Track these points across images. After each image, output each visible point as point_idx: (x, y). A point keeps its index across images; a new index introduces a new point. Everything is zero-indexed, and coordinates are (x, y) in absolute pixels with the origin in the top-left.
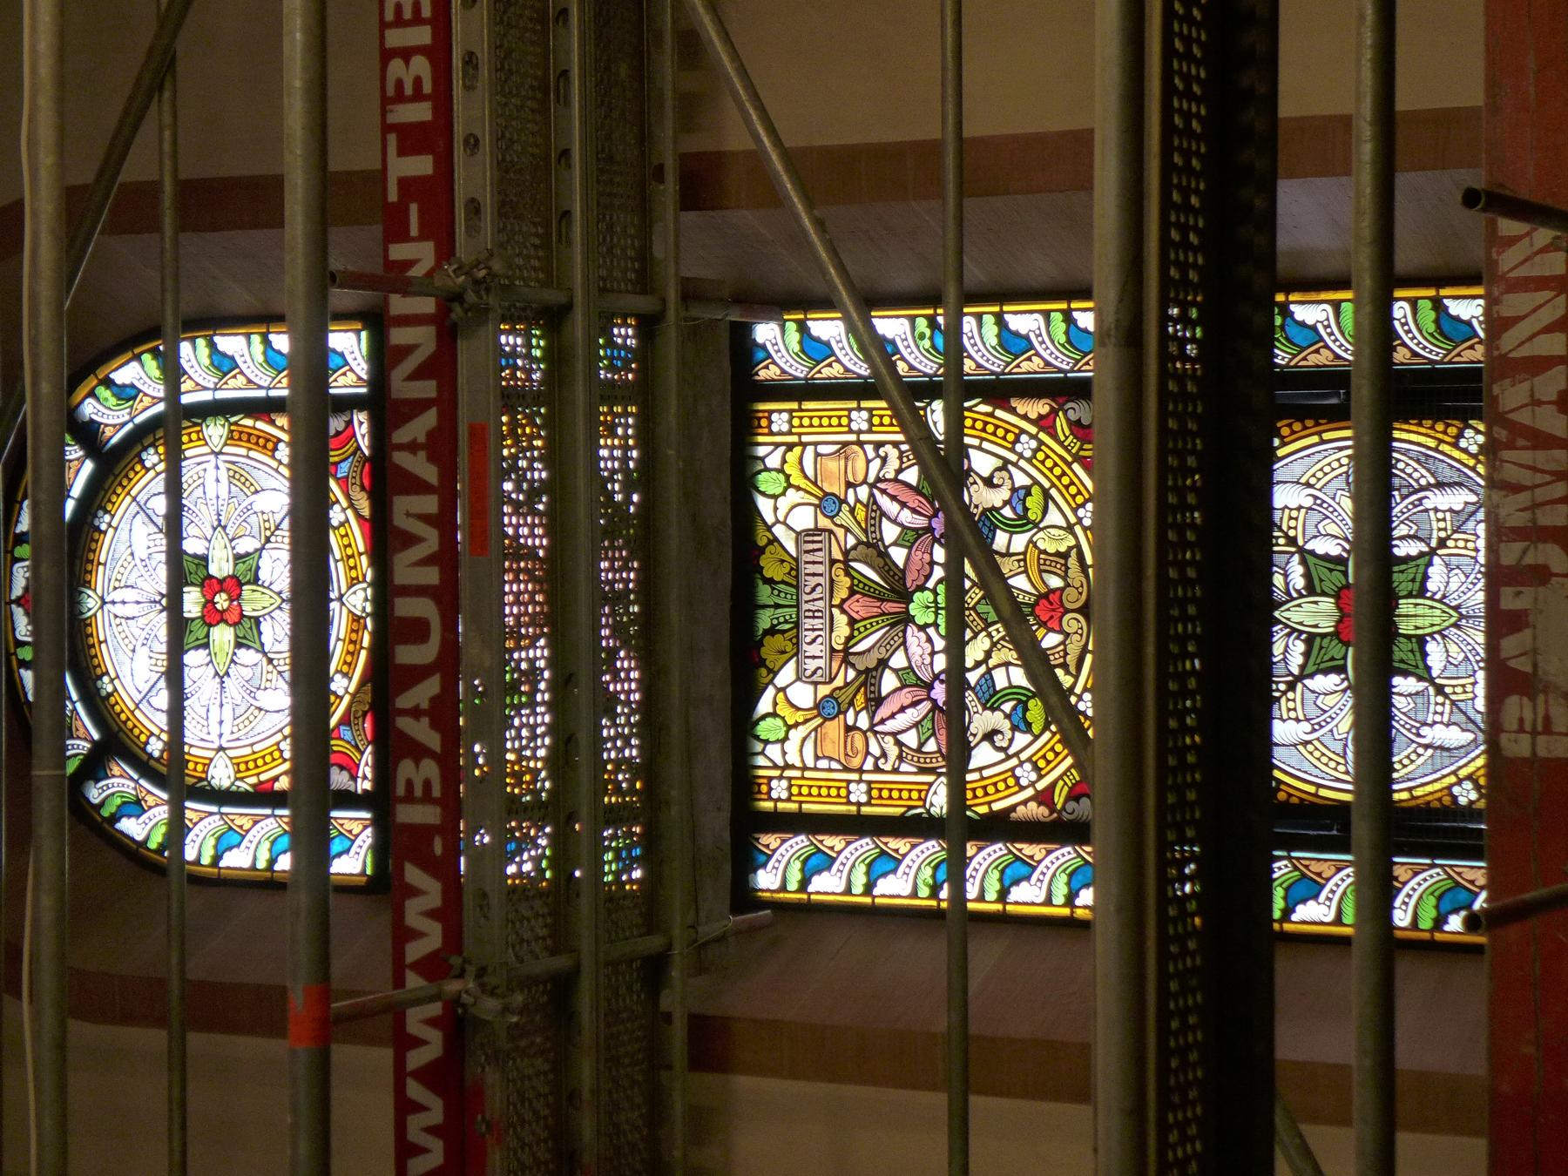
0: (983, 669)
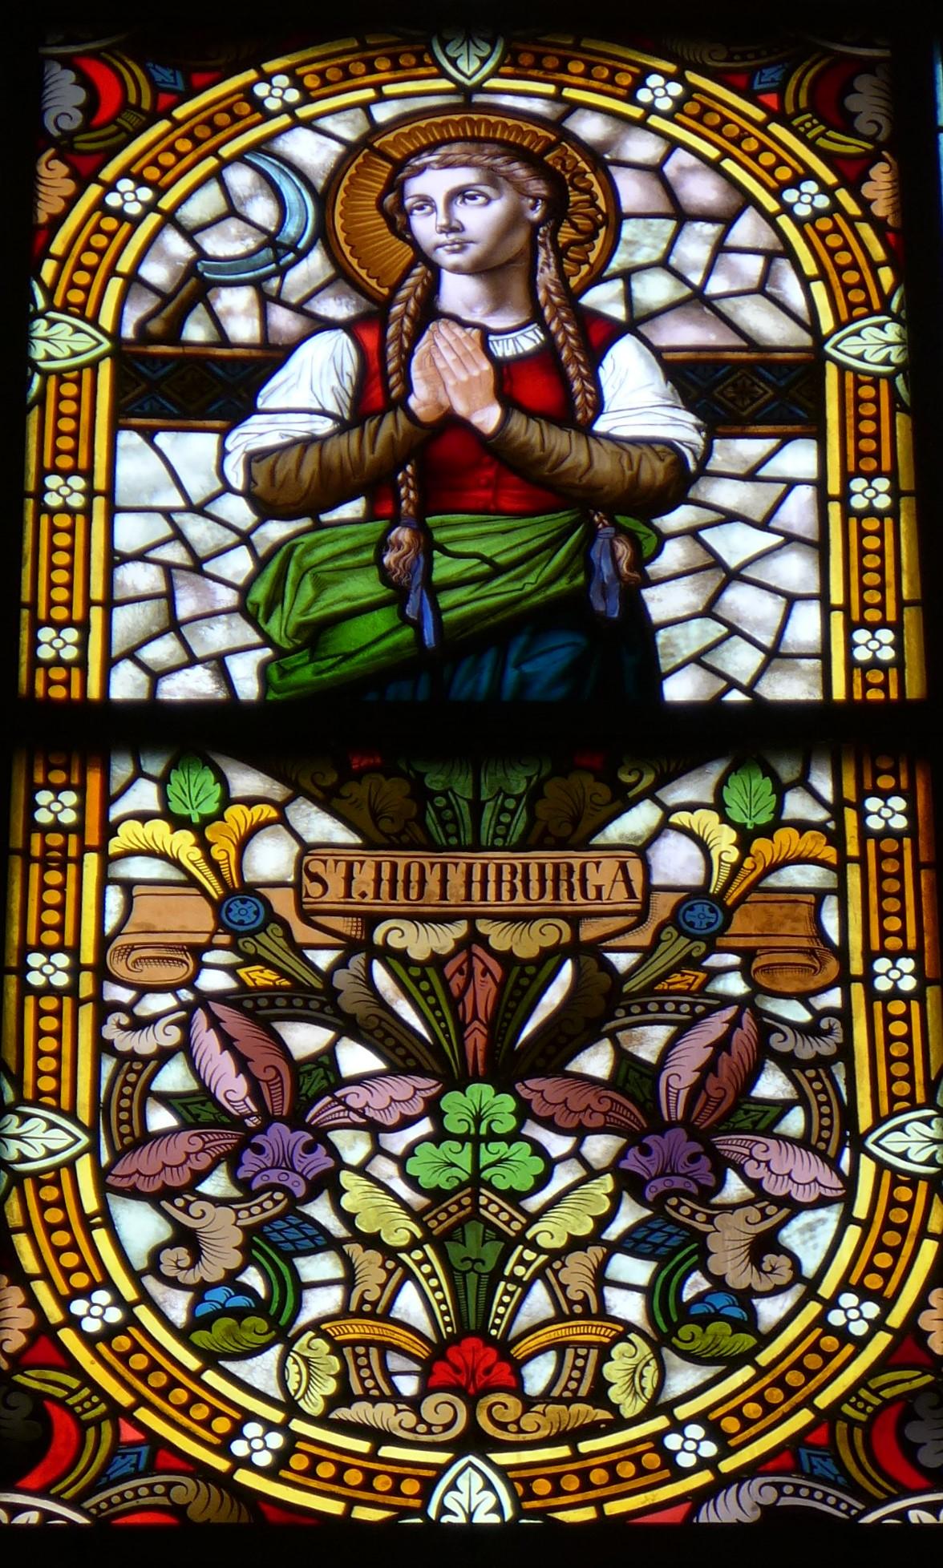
0: (337, 1229)
